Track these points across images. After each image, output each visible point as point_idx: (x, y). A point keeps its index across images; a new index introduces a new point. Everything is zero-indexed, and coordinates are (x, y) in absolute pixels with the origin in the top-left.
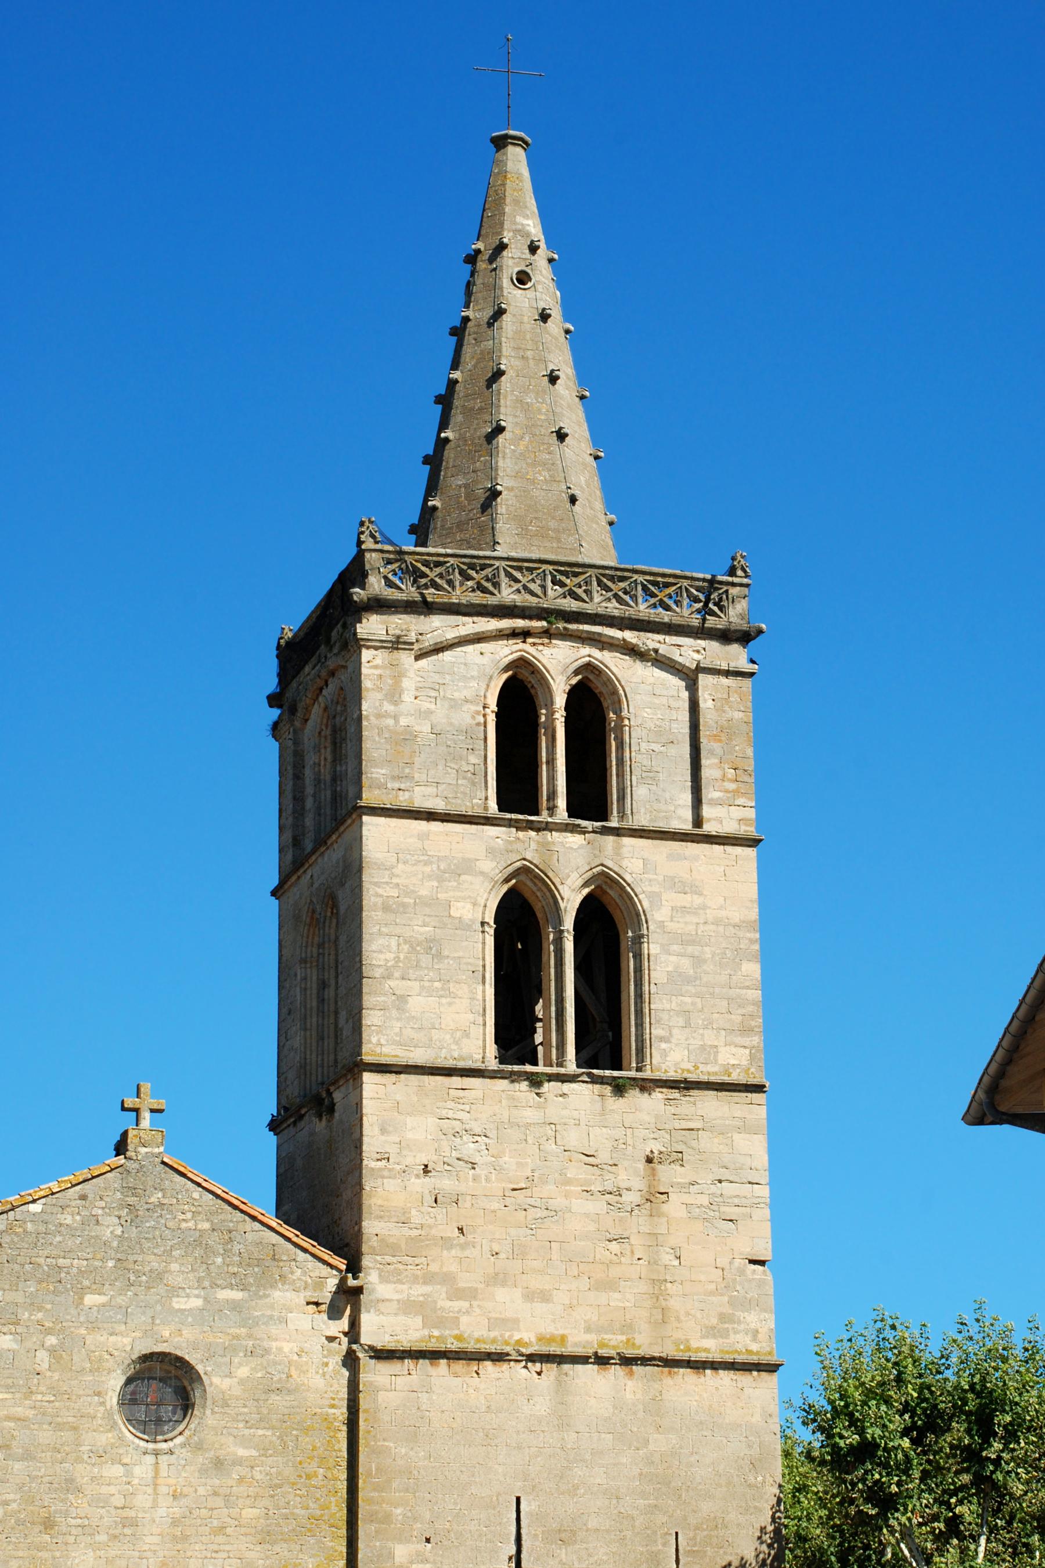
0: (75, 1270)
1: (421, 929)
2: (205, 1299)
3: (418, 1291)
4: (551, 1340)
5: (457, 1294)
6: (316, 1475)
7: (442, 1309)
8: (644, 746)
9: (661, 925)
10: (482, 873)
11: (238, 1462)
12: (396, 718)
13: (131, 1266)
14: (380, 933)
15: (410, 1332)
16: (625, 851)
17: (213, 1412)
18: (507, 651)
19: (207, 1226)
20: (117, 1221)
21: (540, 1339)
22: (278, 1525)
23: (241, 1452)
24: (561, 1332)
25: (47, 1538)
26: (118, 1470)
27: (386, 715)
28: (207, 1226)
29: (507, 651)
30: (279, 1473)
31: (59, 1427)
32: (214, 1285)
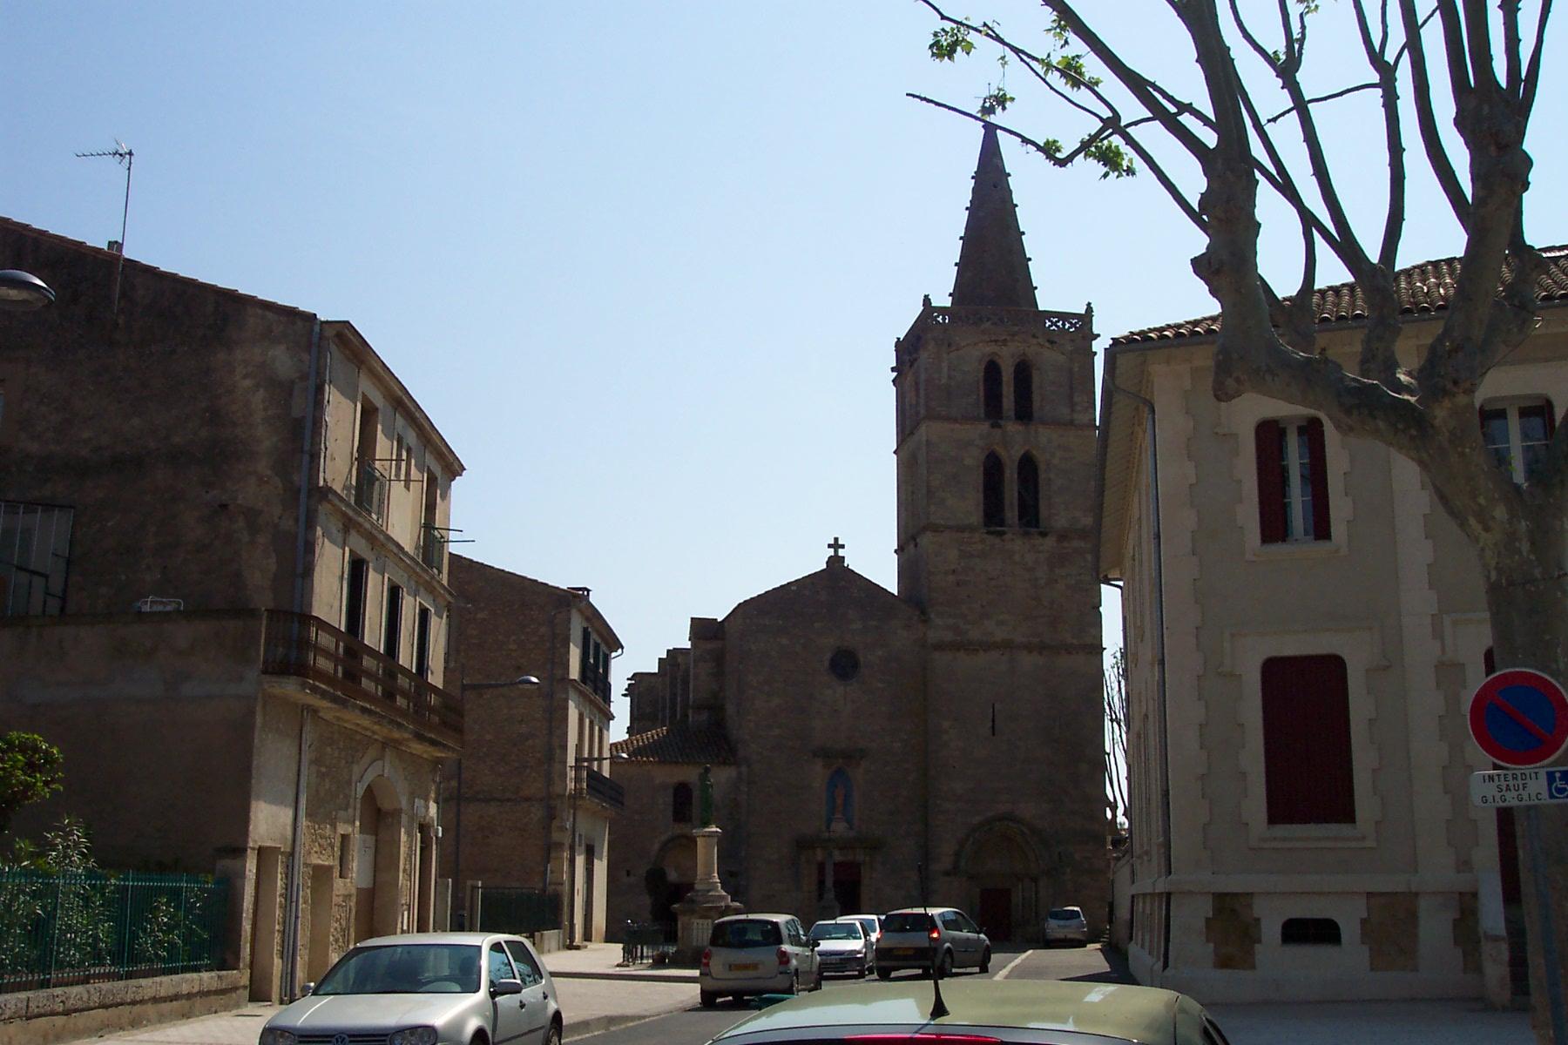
15: (949, 636)
29: (990, 349)
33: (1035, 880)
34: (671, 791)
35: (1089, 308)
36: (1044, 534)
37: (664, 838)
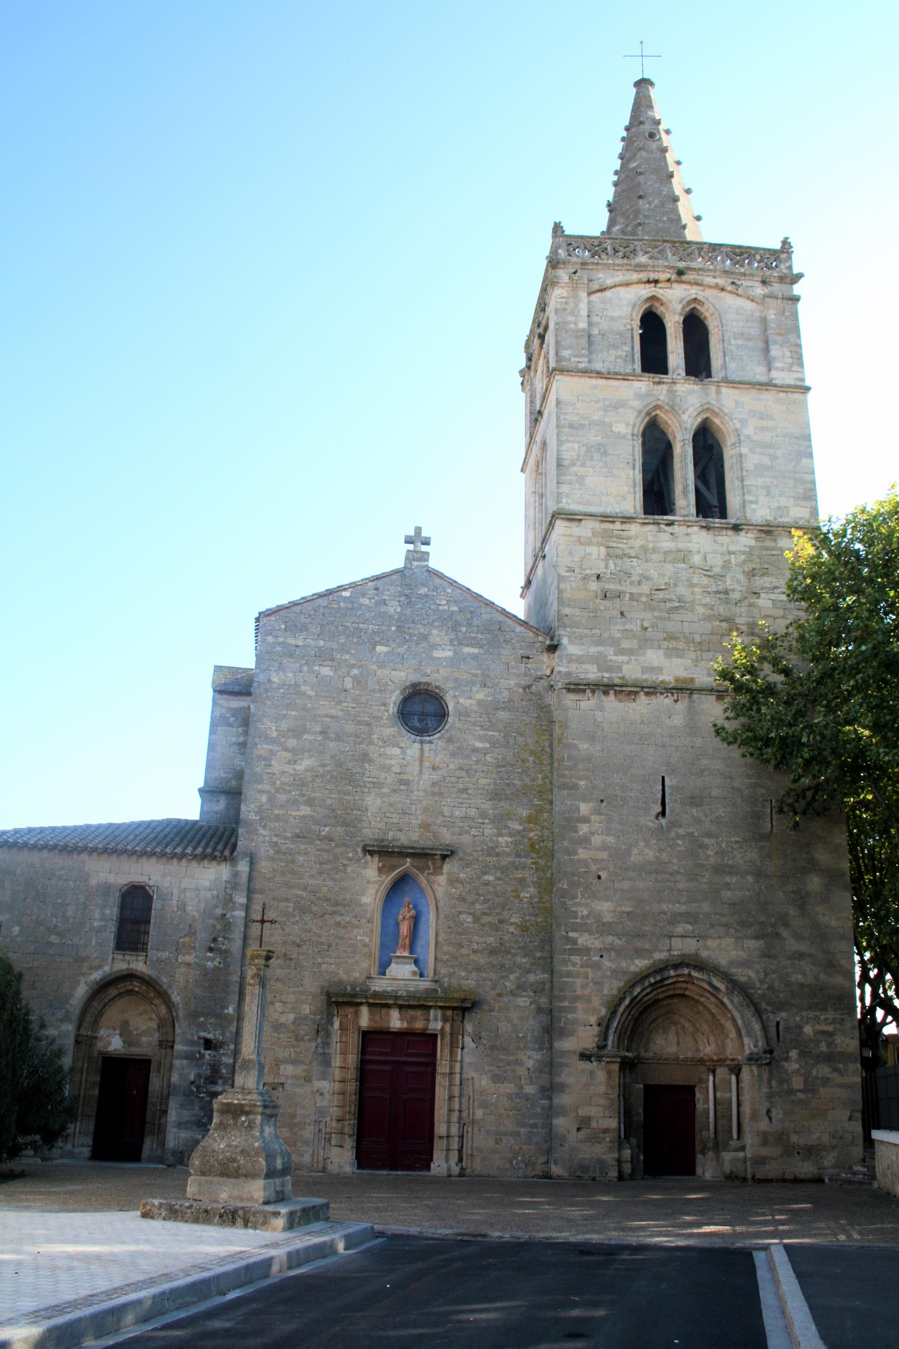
0: (370, 631)
1: (593, 437)
2: (455, 653)
3: (593, 650)
4: (685, 680)
5: (621, 652)
6: (527, 760)
7: (611, 661)
8: (733, 342)
9: (748, 437)
10: (632, 408)
11: (476, 750)
12: (576, 324)
13: (406, 630)
14: (567, 441)
16: (723, 396)
17: (459, 720)
18: (646, 291)
19: (455, 608)
20: (397, 603)
21: (677, 680)
22: (503, 790)
23: (478, 745)
24: (691, 676)
25: (350, 788)
26: (397, 751)
27: (570, 323)
28: (455, 608)
29: (646, 291)
30: (503, 759)
31: (359, 723)
32: (460, 644)
33: (736, 1070)
34: (115, 899)
35: (785, 243)
36: (736, 528)
37: (97, 975)
